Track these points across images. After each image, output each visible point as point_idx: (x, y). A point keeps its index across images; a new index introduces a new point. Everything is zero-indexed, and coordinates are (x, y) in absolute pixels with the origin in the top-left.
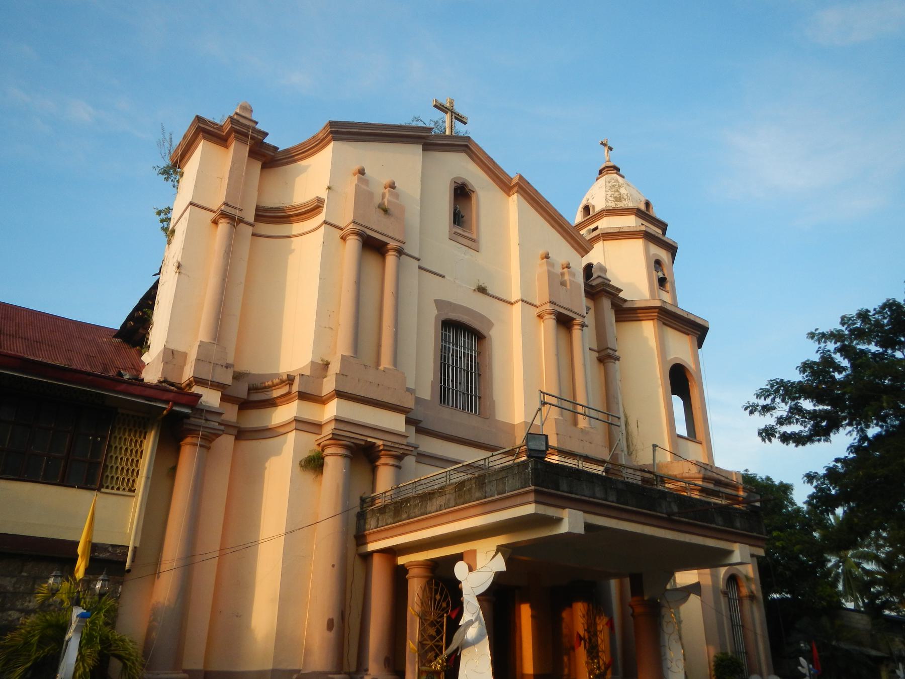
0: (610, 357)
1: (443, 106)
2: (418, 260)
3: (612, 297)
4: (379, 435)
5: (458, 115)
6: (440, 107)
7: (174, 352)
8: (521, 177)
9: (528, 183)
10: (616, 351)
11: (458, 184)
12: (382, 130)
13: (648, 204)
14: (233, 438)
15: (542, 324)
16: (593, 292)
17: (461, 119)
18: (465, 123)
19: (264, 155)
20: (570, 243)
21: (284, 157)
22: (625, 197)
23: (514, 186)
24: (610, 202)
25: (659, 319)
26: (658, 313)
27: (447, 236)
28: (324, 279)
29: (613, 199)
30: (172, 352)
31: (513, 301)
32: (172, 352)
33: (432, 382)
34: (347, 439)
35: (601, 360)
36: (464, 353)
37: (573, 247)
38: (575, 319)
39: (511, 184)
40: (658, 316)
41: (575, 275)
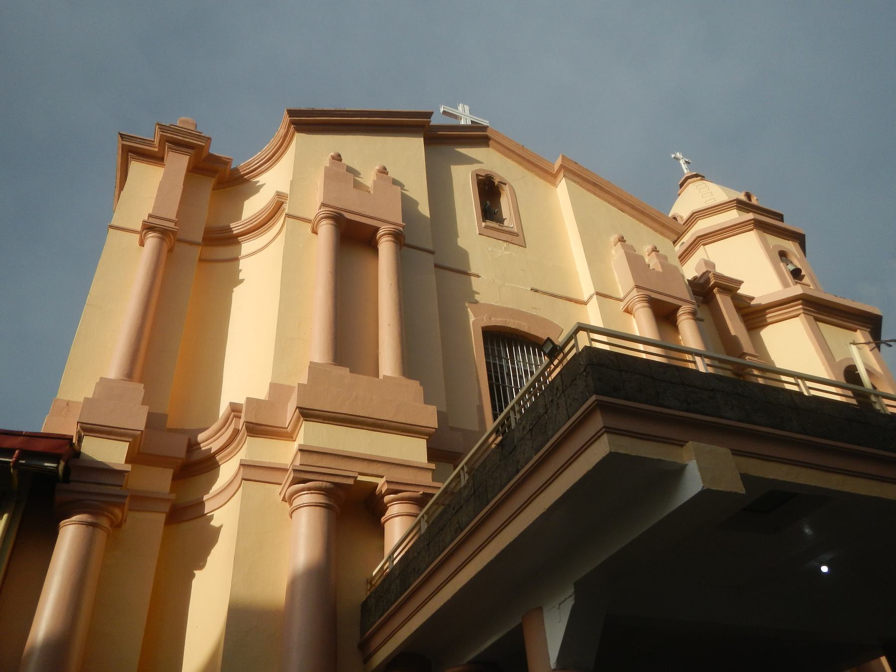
4: (379, 469)
7: (69, 404)
9: (576, 163)
13: (748, 196)
14: (162, 517)
15: (634, 321)
19: (216, 172)
20: (651, 227)
23: (559, 171)
25: (806, 312)
26: (802, 305)
27: (478, 233)
30: (67, 403)
31: (585, 299)
32: (67, 403)
34: (321, 478)
37: (656, 231)
38: (681, 306)
39: (554, 171)
40: (804, 309)
41: (667, 258)
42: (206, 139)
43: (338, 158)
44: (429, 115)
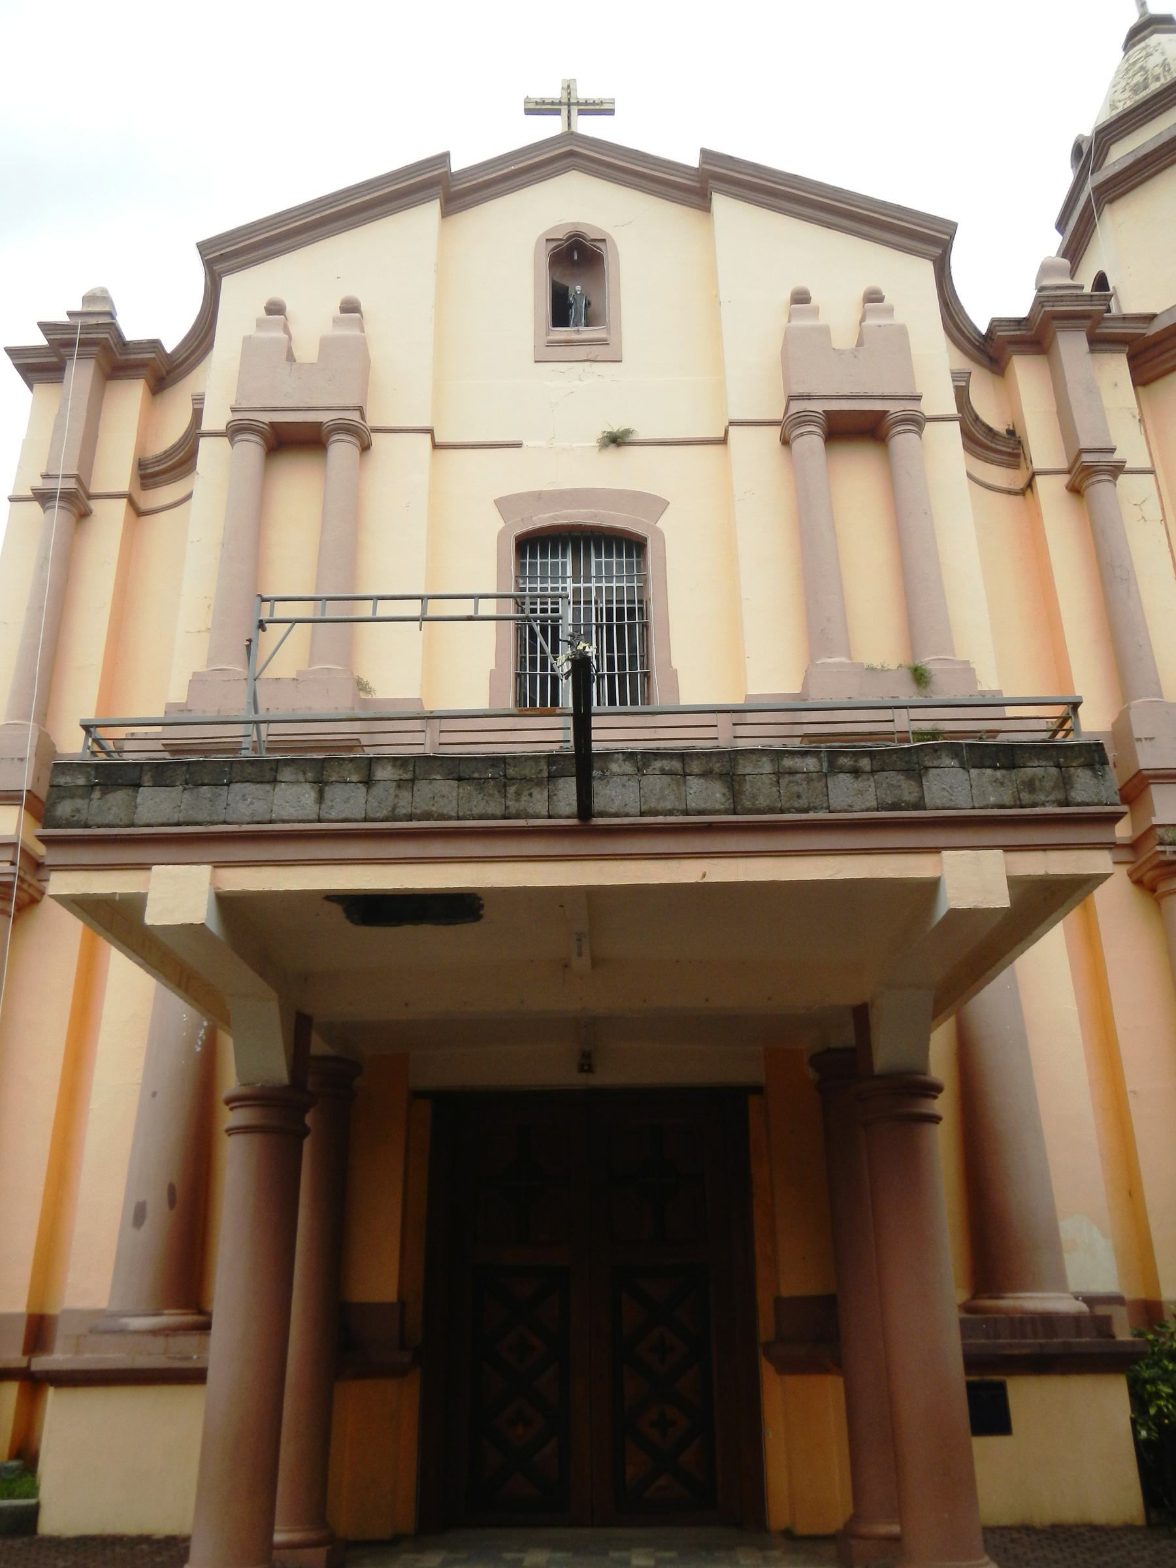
0: (1090, 471)
1: (543, 103)
2: (430, 431)
3: (1088, 323)
5: (586, 103)
6: (537, 108)
8: (706, 155)
9: (731, 158)
10: (1112, 451)
11: (560, 240)
12: (322, 211)
16: (1030, 333)
17: (598, 107)
18: (611, 112)
21: (189, 352)
22: (1158, 70)
24: (1122, 103)
28: (198, 541)
29: (1127, 94)
33: (492, 671)
35: (1075, 490)
36: (599, 589)
42: (109, 327)
43: (275, 309)
44: (445, 158)
